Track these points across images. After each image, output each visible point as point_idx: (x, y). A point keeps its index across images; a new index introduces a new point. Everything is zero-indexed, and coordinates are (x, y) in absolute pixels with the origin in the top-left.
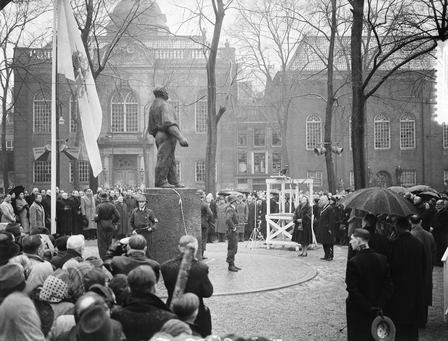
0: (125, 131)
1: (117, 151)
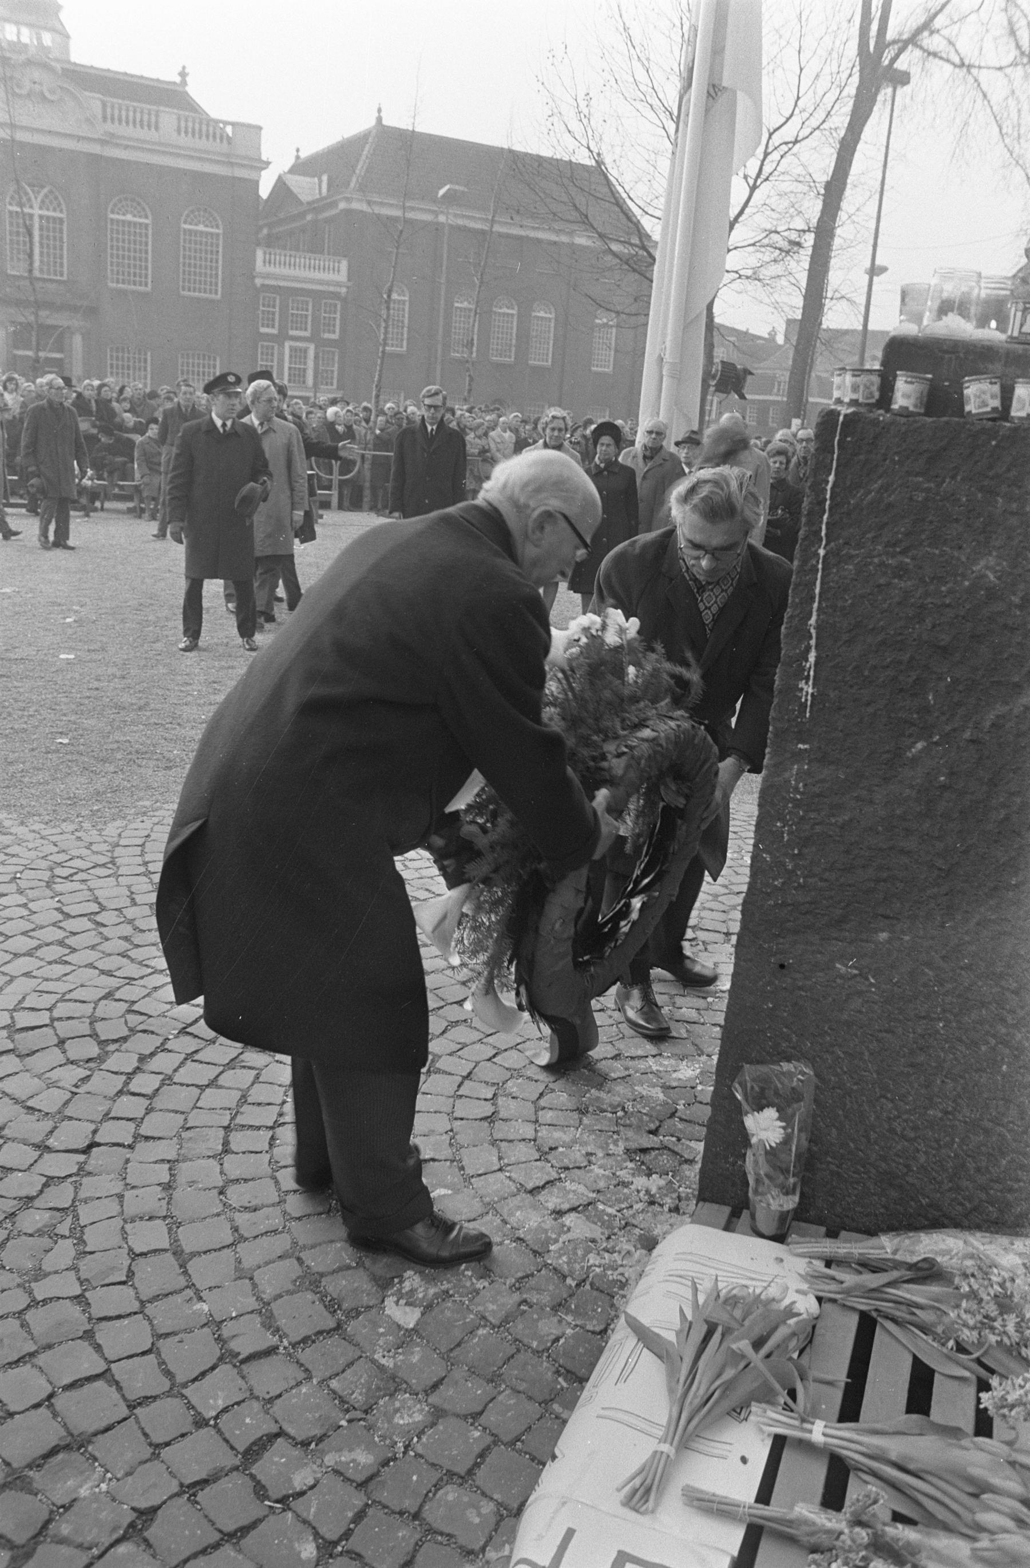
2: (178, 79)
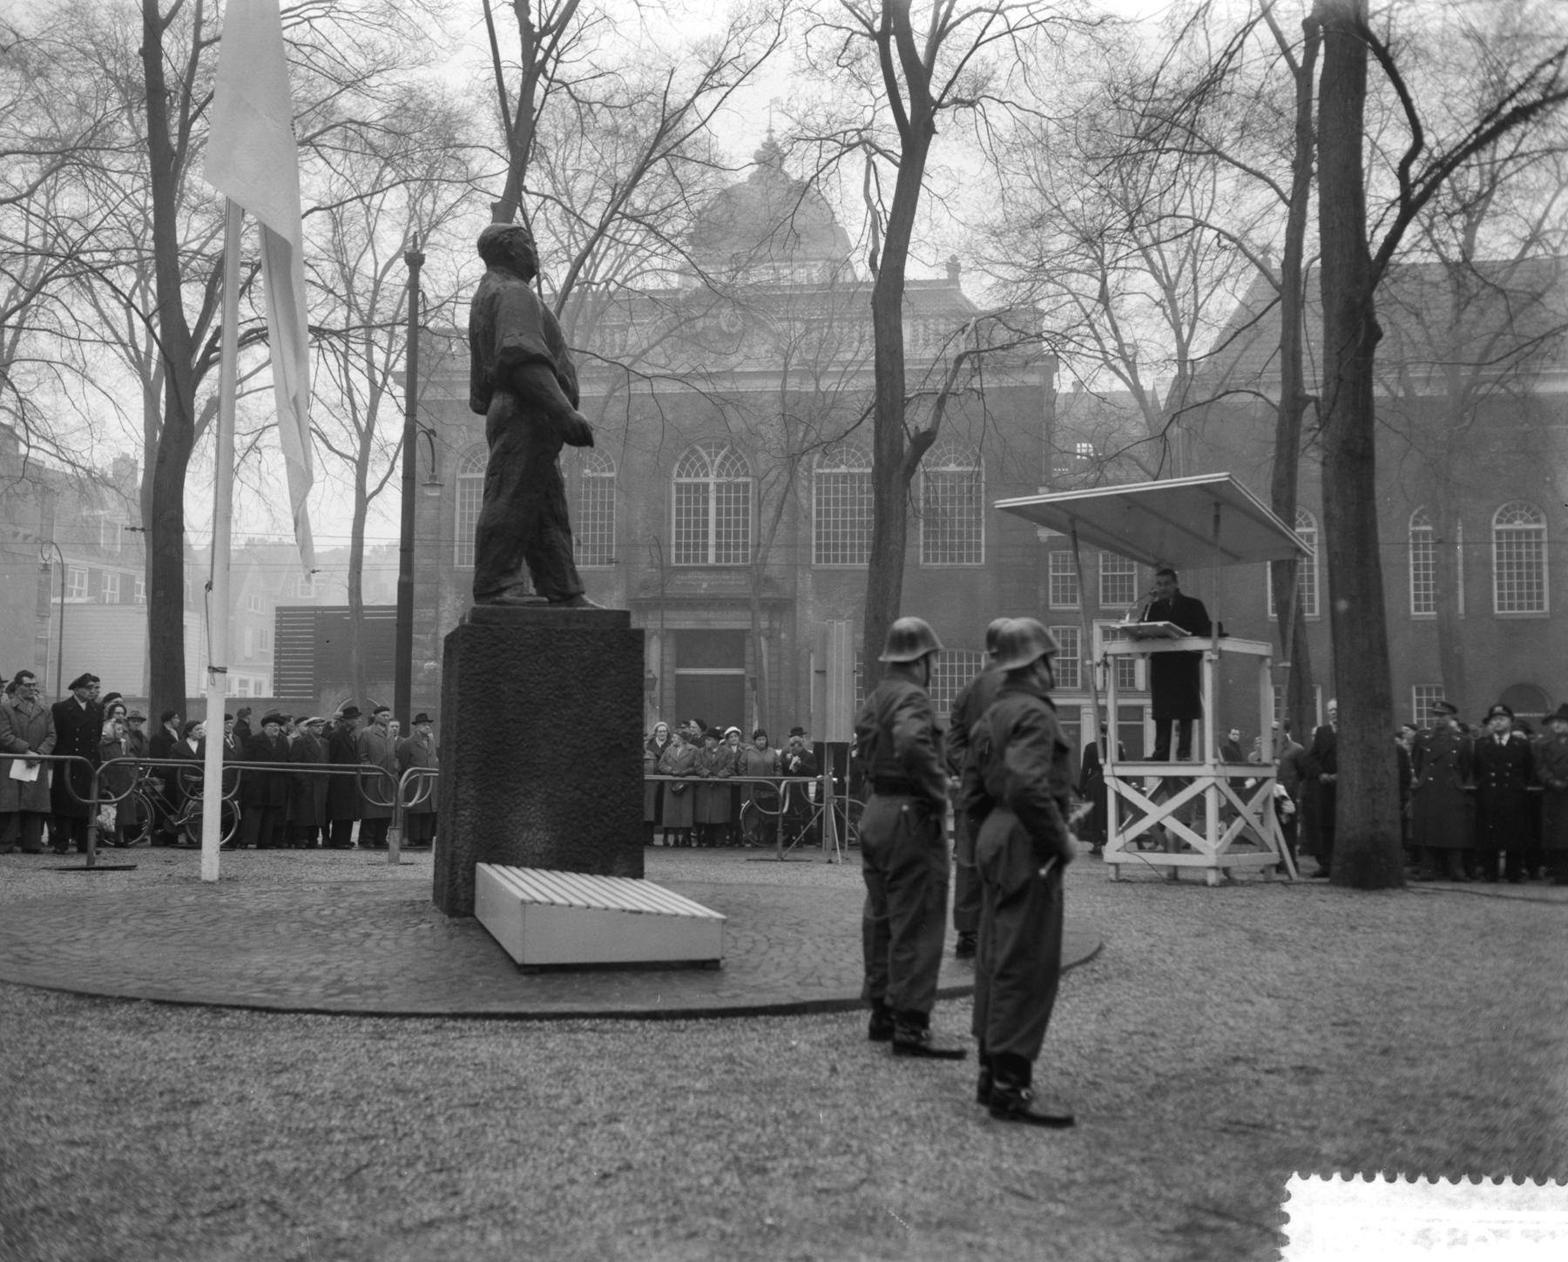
0: (711, 560)
1: (685, 621)
2: (944, 275)
